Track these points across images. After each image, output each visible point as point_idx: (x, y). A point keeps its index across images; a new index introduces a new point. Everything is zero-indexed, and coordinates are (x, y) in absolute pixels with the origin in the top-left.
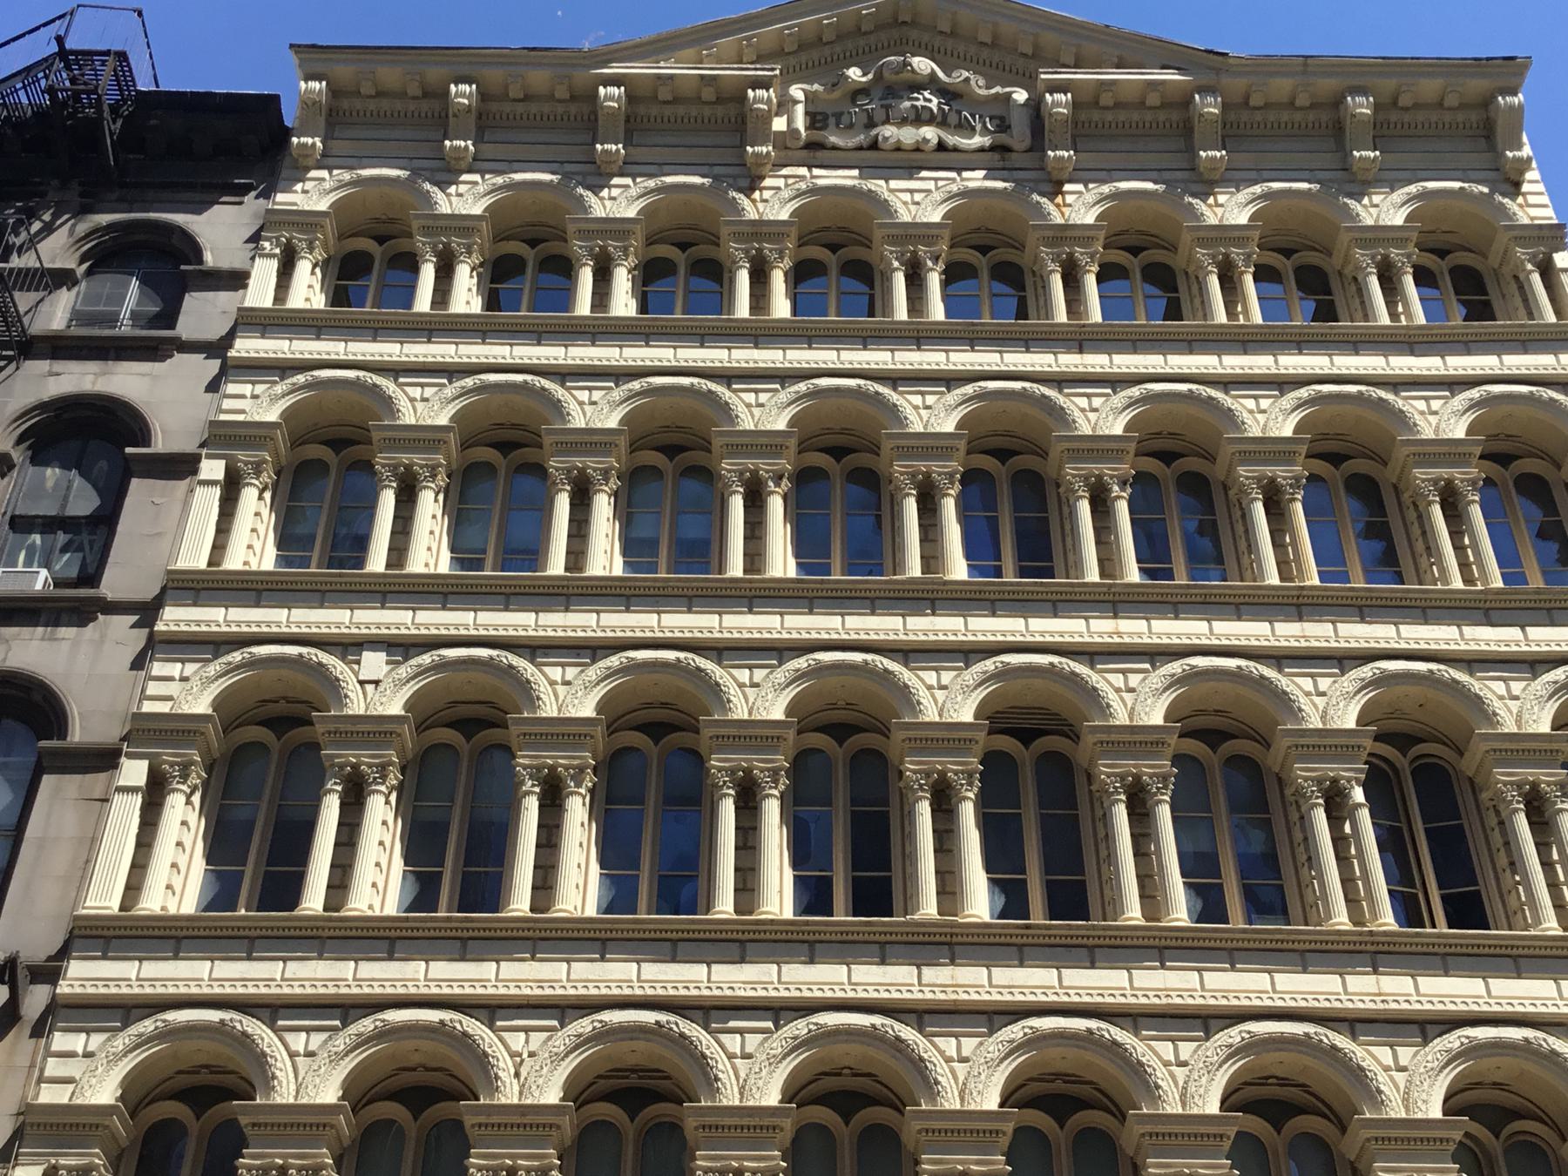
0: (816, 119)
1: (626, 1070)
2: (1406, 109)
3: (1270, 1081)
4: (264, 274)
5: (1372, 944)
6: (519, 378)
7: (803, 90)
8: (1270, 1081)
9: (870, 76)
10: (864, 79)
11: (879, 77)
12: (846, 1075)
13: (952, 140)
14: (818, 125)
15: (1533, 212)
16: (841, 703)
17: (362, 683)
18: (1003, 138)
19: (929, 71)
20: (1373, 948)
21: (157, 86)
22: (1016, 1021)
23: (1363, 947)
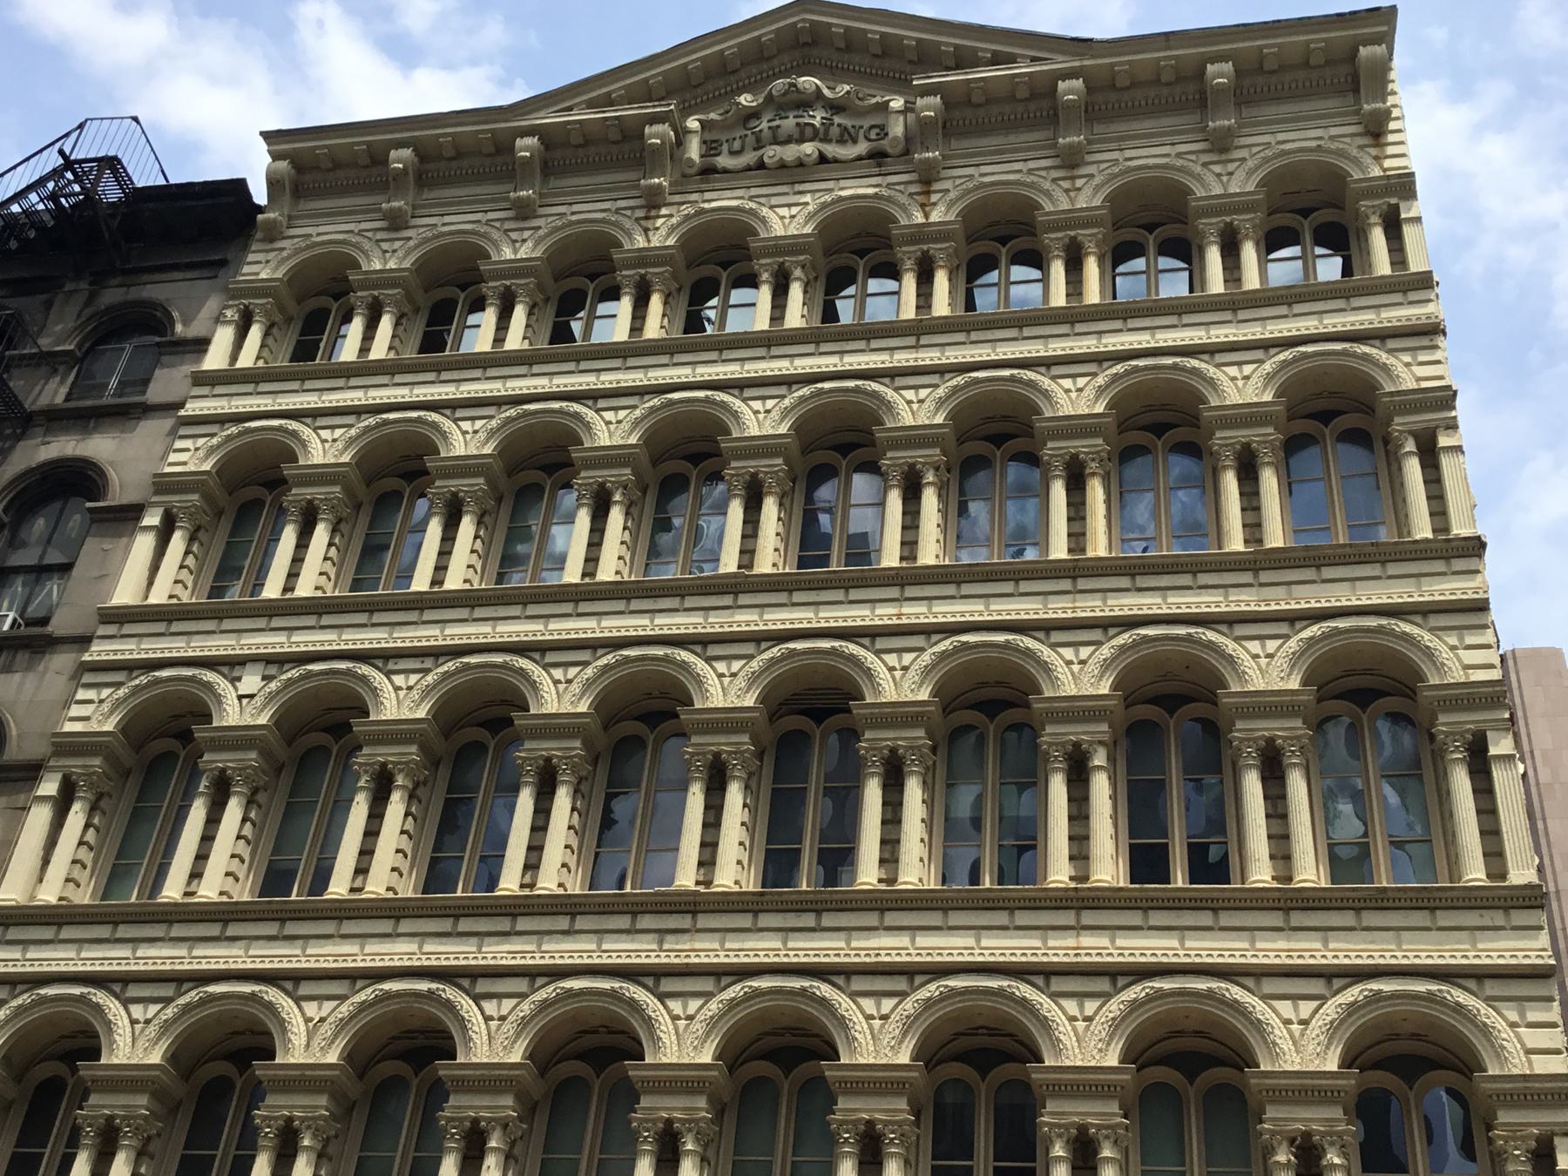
0: (710, 148)
1: (413, 1032)
2: (1273, 72)
4: (223, 337)
6: (701, 394)
7: (698, 120)
10: (754, 104)
13: (831, 150)
15: (1388, 163)
16: (656, 693)
17: (240, 697)
19: (814, 87)
21: (167, 180)
22: (934, 980)
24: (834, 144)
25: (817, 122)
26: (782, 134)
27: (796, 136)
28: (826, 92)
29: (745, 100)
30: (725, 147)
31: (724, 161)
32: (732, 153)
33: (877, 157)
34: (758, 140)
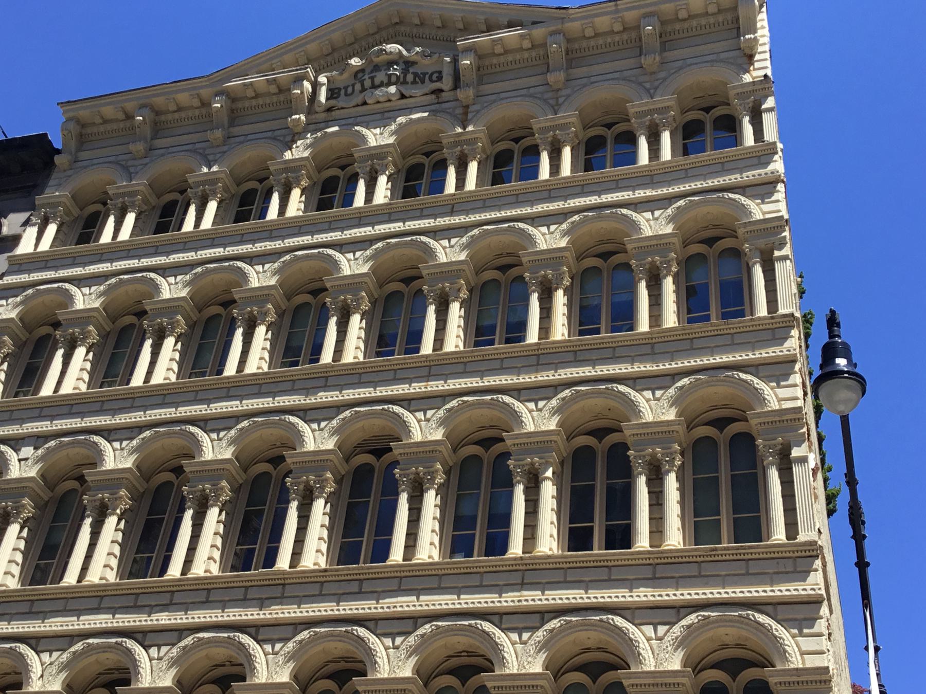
2: (684, 20)
3: (463, 654)
5: (522, 565)
7: (325, 76)
8: (463, 654)
9: (364, 61)
11: (369, 62)
12: (228, 665)
14: (335, 96)
16: (278, 444)
17: (20, 460)
18: (437, 85)
20: (524, 568)
23: (518, 567)
27: (386, 81)
28: (405, 52)
29: (355, 62)
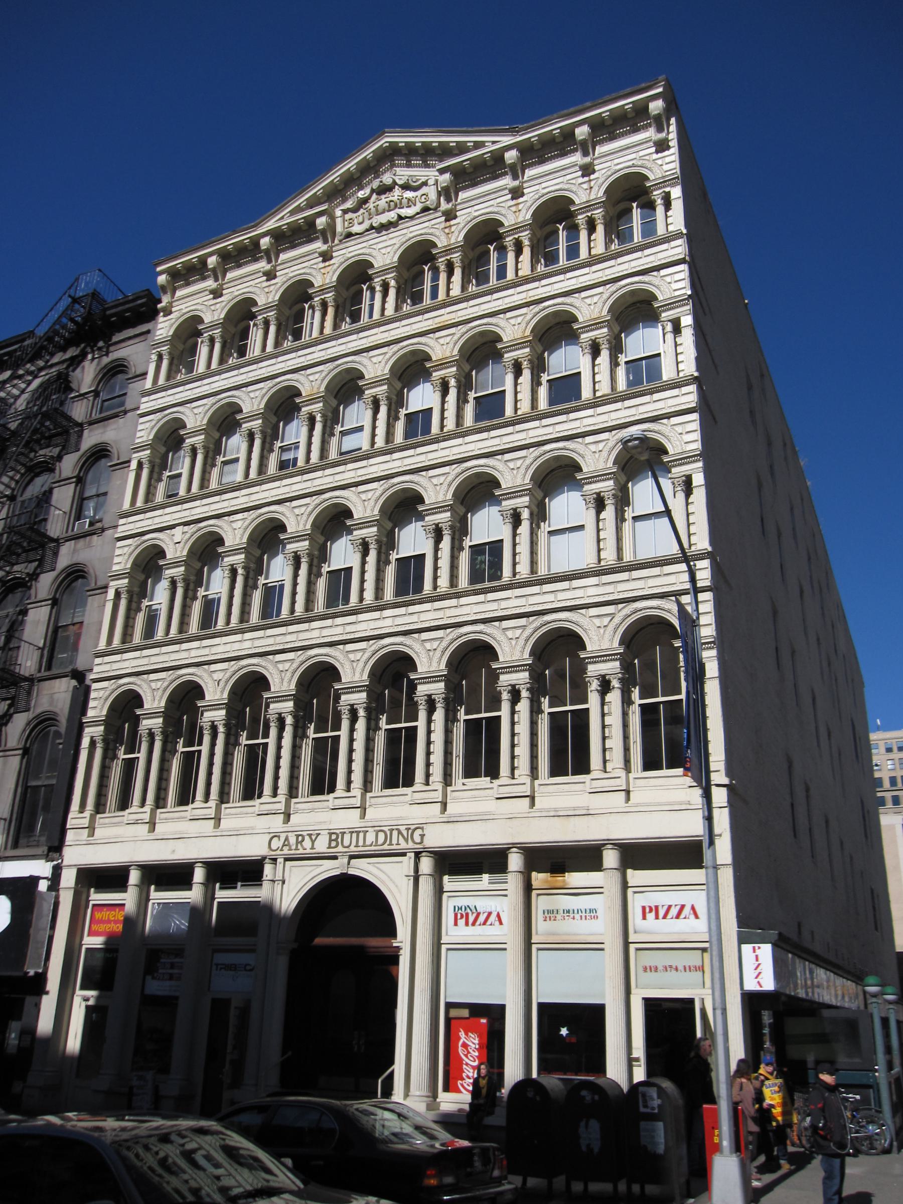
13: (405, 212)
19: (391, 180)
24: (405, 209)
25: (395, 199)
26: (380, 209)
30: (356, 221)
31: (356, 229)
32: (360, 224)
33: (426, 209)
34: (370, 214)
